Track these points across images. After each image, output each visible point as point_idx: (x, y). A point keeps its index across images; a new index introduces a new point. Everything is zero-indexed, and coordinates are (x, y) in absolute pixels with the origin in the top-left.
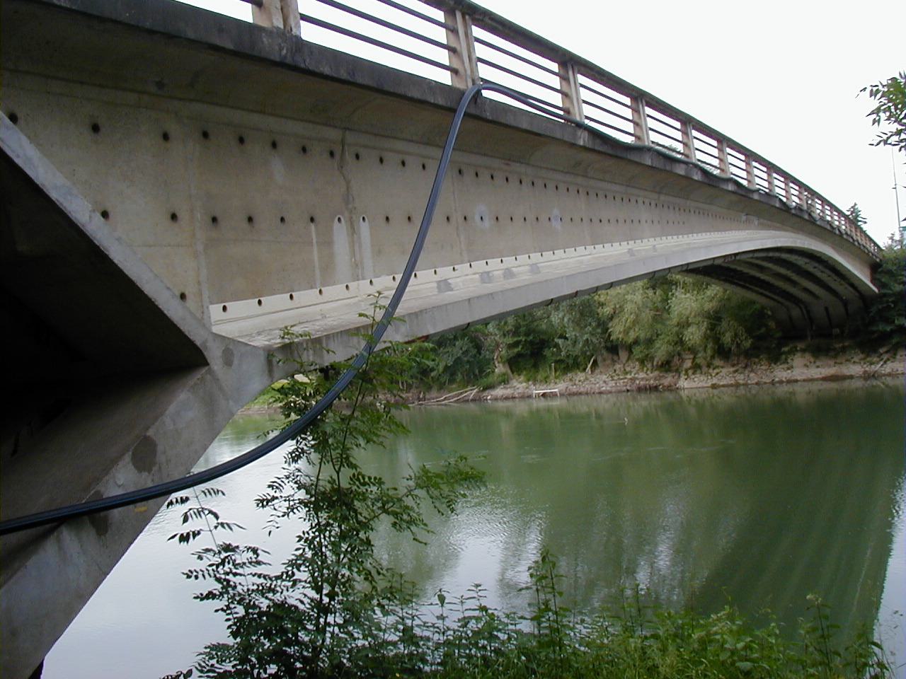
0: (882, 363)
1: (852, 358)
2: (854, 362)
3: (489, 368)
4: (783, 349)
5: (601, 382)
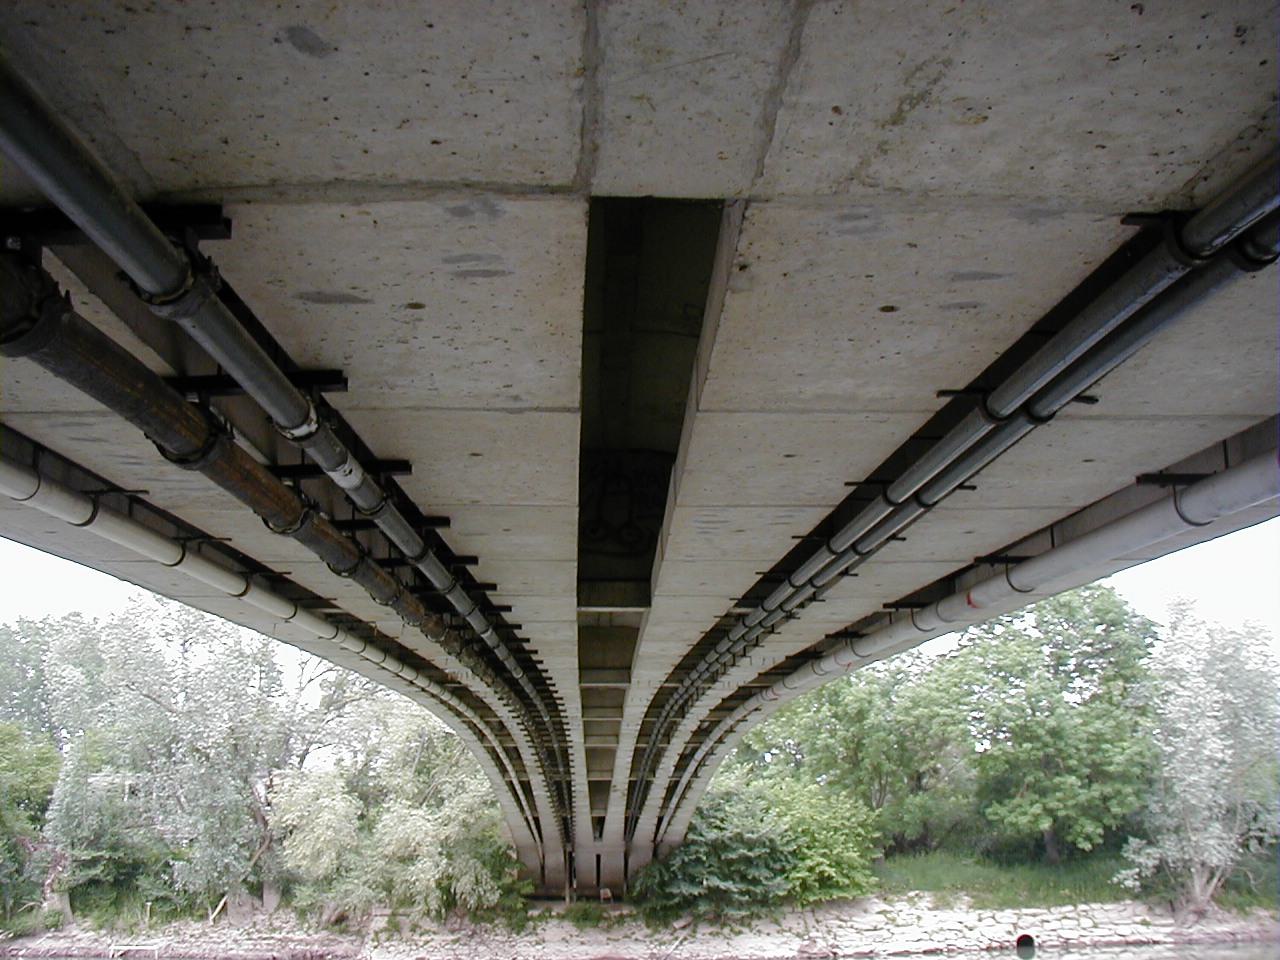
0: (677, 943)
1: (633, 933)
2: (636, 940)
3: (33, 900)
4: (530, 913)
5: (229, 942)
